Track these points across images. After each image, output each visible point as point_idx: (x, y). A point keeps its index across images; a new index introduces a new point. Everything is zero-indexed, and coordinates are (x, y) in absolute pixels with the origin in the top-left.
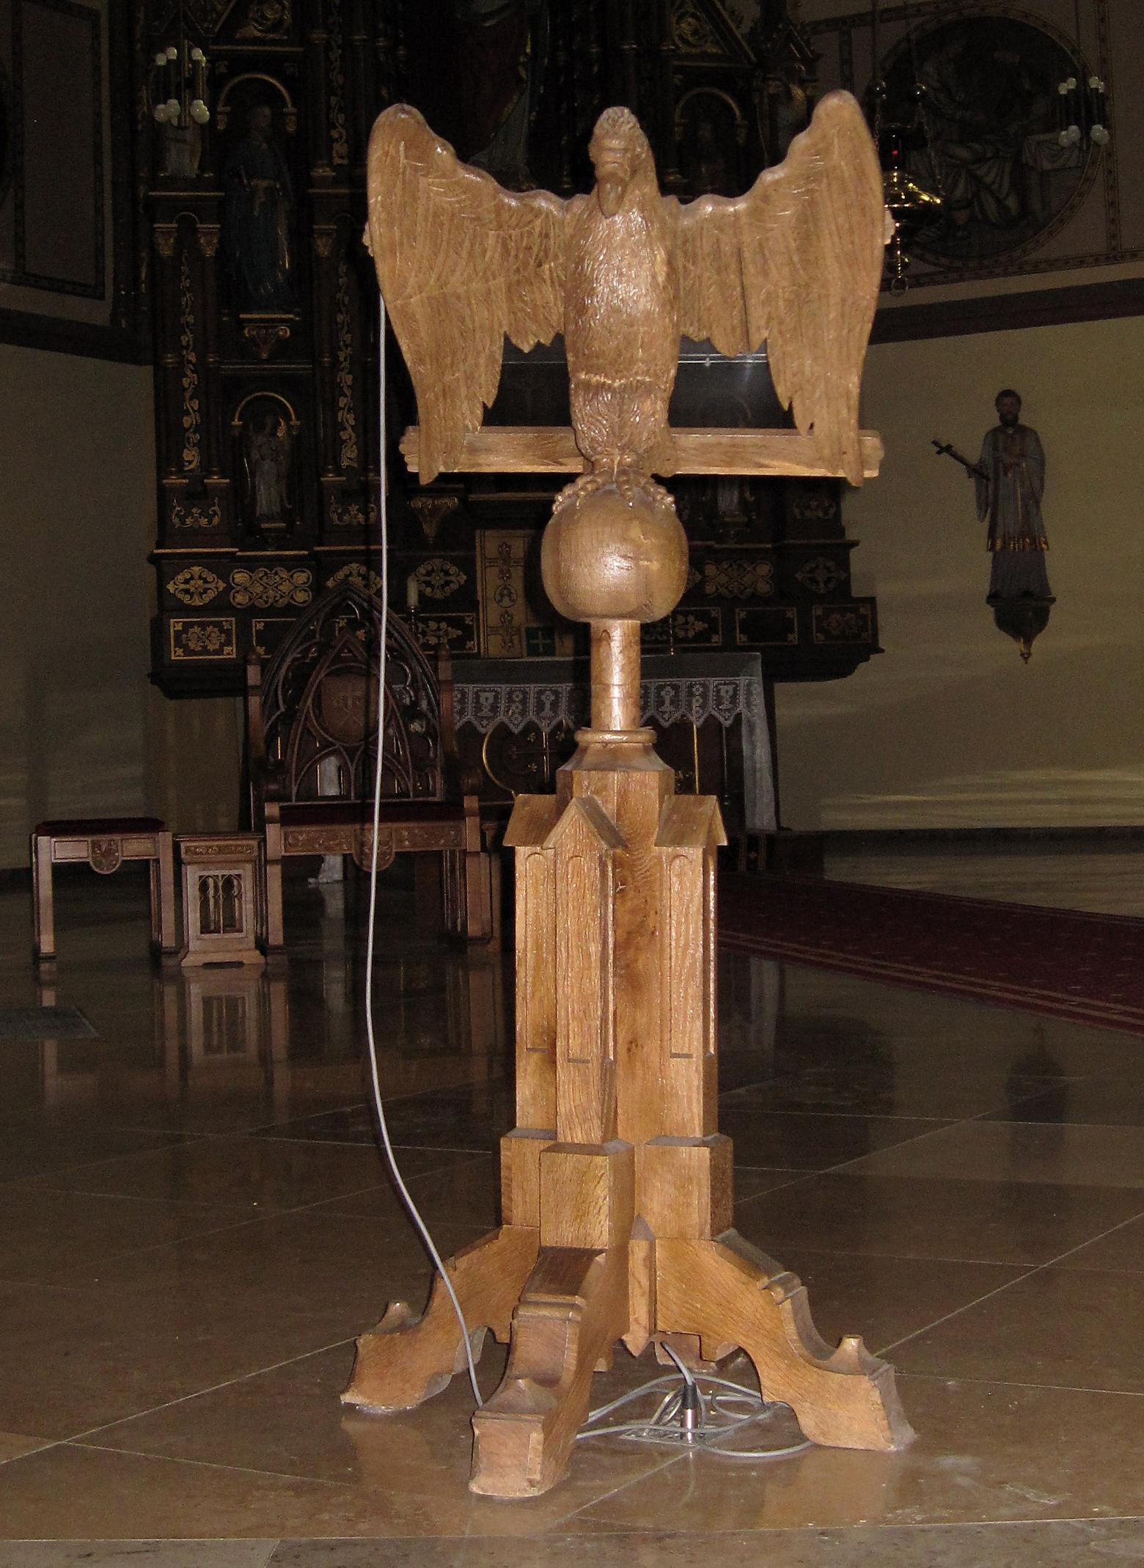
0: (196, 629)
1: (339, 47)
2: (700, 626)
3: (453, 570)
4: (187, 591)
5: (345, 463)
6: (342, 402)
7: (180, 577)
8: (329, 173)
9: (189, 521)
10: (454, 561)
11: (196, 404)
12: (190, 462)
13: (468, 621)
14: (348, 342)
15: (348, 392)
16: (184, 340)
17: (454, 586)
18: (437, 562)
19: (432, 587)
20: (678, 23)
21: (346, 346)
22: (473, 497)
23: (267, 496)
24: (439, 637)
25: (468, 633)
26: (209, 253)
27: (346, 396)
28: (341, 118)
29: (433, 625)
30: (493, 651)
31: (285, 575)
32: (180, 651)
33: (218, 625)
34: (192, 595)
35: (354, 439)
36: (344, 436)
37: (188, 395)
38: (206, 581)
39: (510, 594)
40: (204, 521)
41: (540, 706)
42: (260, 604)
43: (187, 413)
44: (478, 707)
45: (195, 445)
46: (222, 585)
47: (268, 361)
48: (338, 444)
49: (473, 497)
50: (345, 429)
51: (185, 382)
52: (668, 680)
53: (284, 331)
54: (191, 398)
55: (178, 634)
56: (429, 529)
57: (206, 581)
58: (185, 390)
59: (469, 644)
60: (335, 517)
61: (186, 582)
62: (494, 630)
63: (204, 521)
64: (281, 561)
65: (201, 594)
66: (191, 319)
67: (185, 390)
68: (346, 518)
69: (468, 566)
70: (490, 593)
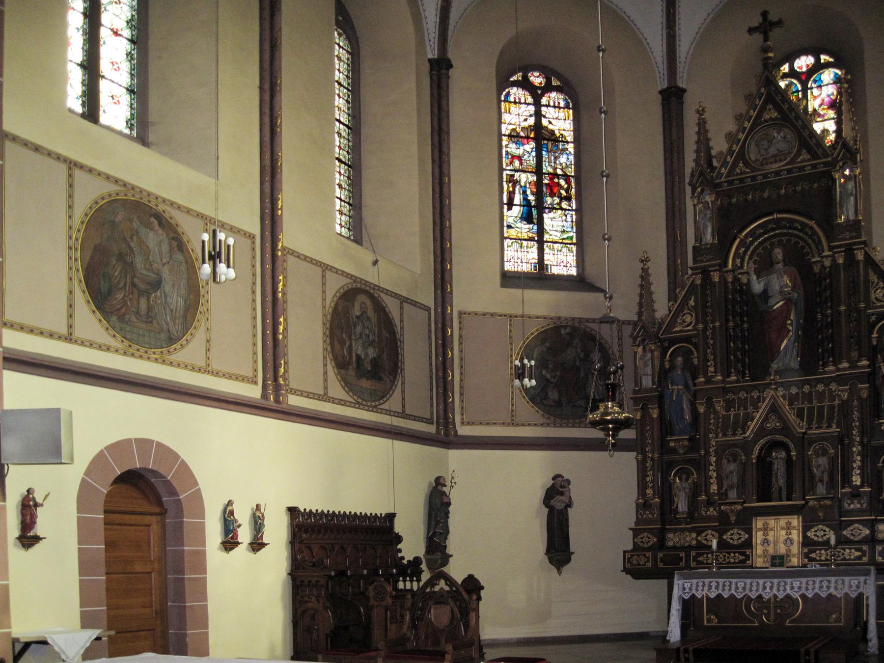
0: (635, 557)
1: (711, 329)
2: (858, 554)
3: (742, 533)
4: (642, 542)
5: (712, 491)
6: (711, 468)
7: (639, 537)
8: (702, 379)
9: (644, 516)
10: (743, 530)
11: (651, 472)
12: (649, 494)
13: (748, 553)
14: (714, 445)
15: (714, 464)
16: (647, 449)
17: (743, 540)
18: (736, 530)
19: (733, 540)
20: (874, 292)
21: (713, 446)
22: (745, 505)
23: (682, 505)
24: (735, 559)
25: (747, 557)
26: (655, 416)
27: (712, 465)
28: (712, 357)
29: (732, 555)
30: (758, 565)
31: (687, 534)
32: (629, 565)
33: (645, 555)
34: (643, 543)
35: (716, 482)
36: (712, 481)
37: (648, 469)
38: (649, 538)
39: (767, 542)
40: (650, 516)
41: (765, 588)
42: (678, 545)
43: (648, 476)
44: (737, 588)
45: (651, 488)
46: (699, 538)
47: (683, 454)
48: (707, 485)
49: (745, 505)
50: (712, 478)
51: (647, 465)
52: (825, 578)
53: (686, 443)
54: (650, 471)
55: (629, 559)
56: (733, 519)
57: (649, 538)
58: (647, 467)
59: (748, 562)
60: (704, 513)
61: (642, 538)
62: (760, 556)
63: (650, 516)
64: (686, 529)
65: (647, 543)
66: (650, 441)
67: (647, 467)
68: (708, 513)
69: (749, 531)
70: (759, 541)
